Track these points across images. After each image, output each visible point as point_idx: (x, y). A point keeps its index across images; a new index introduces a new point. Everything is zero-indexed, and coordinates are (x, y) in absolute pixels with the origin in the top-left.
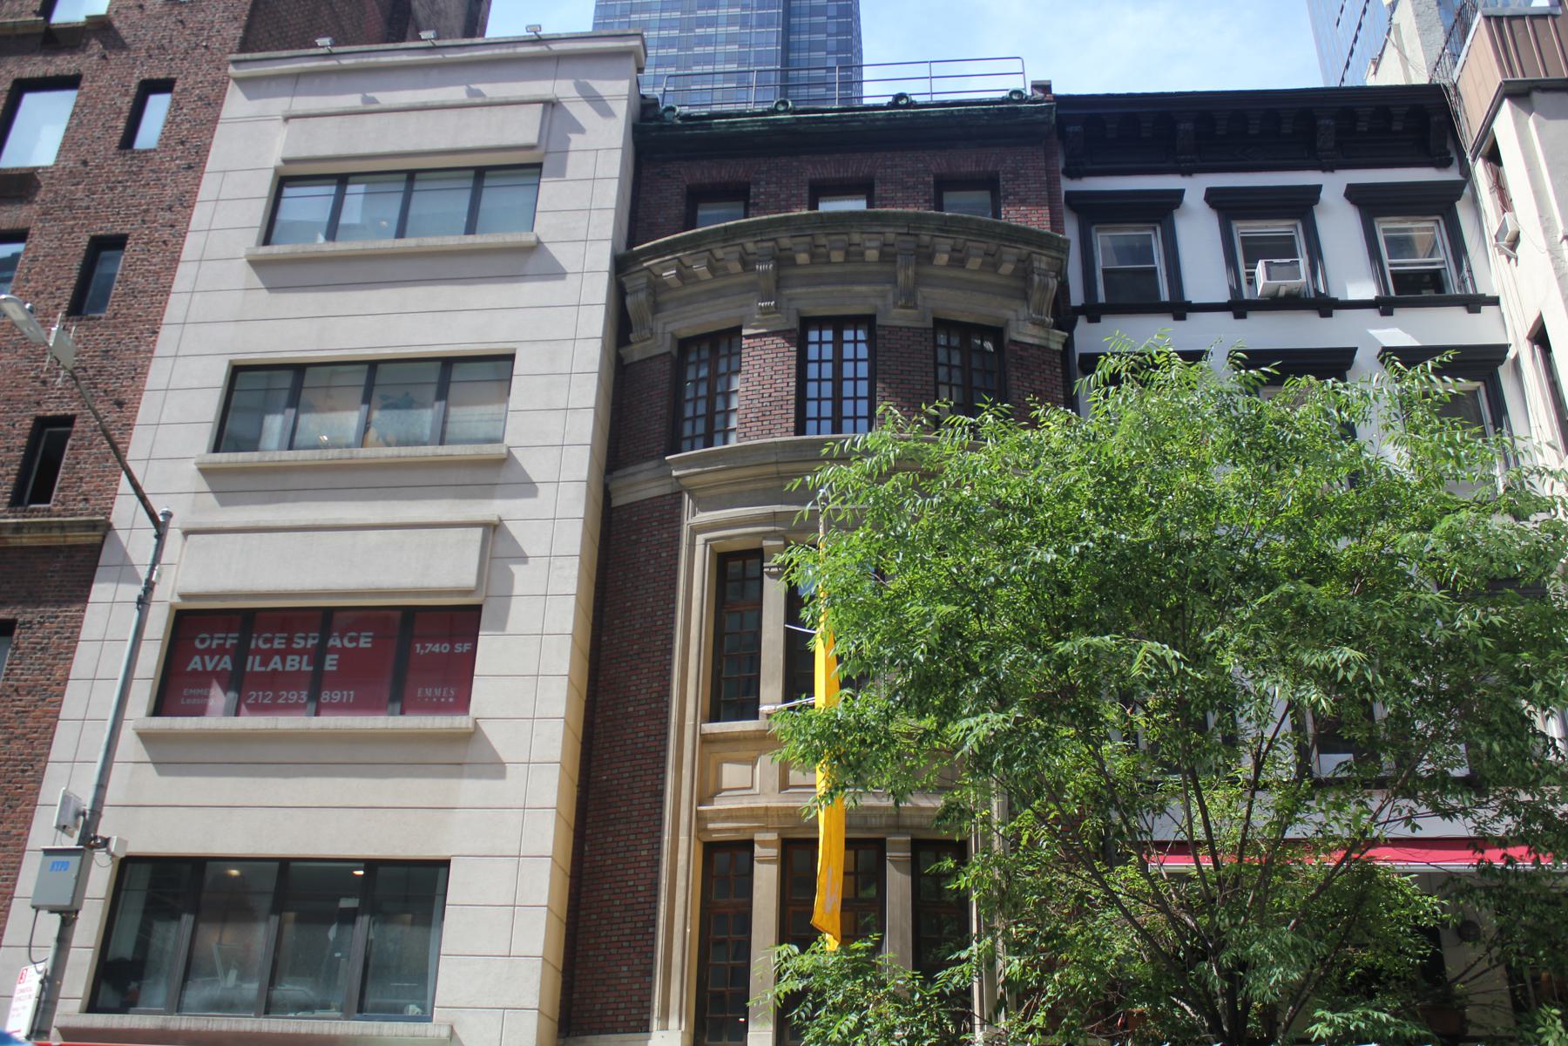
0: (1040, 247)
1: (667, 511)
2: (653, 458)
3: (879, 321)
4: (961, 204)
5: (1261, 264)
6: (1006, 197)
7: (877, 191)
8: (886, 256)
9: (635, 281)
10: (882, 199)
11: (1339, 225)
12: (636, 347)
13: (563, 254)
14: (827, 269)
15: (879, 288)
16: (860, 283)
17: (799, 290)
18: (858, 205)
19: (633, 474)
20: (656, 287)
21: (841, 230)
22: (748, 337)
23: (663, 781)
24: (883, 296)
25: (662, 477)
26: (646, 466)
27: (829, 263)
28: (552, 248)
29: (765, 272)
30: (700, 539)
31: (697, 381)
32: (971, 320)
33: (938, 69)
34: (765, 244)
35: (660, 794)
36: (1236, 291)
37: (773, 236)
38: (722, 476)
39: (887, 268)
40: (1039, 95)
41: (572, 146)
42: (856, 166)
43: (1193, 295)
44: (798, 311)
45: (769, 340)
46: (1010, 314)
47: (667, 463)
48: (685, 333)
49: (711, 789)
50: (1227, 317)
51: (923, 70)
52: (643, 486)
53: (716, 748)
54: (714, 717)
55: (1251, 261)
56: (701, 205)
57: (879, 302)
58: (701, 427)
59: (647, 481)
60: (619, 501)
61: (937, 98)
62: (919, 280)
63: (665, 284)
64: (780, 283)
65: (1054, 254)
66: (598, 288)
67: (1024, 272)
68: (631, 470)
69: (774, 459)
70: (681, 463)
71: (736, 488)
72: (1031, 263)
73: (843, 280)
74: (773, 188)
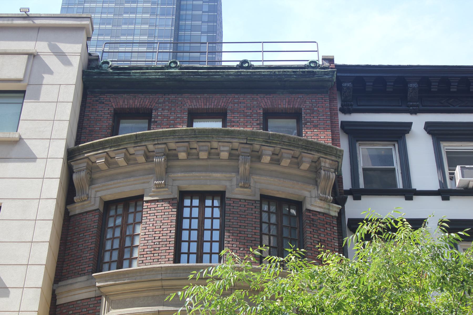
0: (326, 154)
2: (84, 274)
3: (227, 195)
4: (278, 126)
5: (458, 168)
6: (306, 124)
7: (229, 117)
8: (233, 156)
9: (80, 164)
10: (232, 122)
13: (36, 147)
14: (197, 163)
15: (228, 175)
16: (216, 171)
17: (179, 175)
18: (217, 125)
19: (71, 284)
20: (92, 169)
21: (206, 139)
22: (147, 202)
25: (89, 287)
26: (80, 279)
27: (198, 159)
28: (27, 142)
29: (160, 163)
31: (115, 227)
32: (283, 196)
36: (443, 183)
38: (126, 287)
39: (233, 163)
40: (327, 64)
41: (44, 82)
42: (216, 101)
43: (417, 185)
45: (160, 204)
46: (306, 194)
47: (93, 278)
48: (108, 198)
50: (438, 199)
55: (452, 165)
56: (122, 121)
57: (228, 184)
58: (115, 256)
60: (60, 301)
61: (266, 64)
62: (252, 171)
63: (98, 167)
64: (168, 170)
65: (334, 158)
66: (56, 168)
67: (316, 169)
68: (70, 281)
69: (160, 277)
70: (103, 278)
71: (136, 295)
72: (320, 163)
73: (207, 169)
74: (166, 113)
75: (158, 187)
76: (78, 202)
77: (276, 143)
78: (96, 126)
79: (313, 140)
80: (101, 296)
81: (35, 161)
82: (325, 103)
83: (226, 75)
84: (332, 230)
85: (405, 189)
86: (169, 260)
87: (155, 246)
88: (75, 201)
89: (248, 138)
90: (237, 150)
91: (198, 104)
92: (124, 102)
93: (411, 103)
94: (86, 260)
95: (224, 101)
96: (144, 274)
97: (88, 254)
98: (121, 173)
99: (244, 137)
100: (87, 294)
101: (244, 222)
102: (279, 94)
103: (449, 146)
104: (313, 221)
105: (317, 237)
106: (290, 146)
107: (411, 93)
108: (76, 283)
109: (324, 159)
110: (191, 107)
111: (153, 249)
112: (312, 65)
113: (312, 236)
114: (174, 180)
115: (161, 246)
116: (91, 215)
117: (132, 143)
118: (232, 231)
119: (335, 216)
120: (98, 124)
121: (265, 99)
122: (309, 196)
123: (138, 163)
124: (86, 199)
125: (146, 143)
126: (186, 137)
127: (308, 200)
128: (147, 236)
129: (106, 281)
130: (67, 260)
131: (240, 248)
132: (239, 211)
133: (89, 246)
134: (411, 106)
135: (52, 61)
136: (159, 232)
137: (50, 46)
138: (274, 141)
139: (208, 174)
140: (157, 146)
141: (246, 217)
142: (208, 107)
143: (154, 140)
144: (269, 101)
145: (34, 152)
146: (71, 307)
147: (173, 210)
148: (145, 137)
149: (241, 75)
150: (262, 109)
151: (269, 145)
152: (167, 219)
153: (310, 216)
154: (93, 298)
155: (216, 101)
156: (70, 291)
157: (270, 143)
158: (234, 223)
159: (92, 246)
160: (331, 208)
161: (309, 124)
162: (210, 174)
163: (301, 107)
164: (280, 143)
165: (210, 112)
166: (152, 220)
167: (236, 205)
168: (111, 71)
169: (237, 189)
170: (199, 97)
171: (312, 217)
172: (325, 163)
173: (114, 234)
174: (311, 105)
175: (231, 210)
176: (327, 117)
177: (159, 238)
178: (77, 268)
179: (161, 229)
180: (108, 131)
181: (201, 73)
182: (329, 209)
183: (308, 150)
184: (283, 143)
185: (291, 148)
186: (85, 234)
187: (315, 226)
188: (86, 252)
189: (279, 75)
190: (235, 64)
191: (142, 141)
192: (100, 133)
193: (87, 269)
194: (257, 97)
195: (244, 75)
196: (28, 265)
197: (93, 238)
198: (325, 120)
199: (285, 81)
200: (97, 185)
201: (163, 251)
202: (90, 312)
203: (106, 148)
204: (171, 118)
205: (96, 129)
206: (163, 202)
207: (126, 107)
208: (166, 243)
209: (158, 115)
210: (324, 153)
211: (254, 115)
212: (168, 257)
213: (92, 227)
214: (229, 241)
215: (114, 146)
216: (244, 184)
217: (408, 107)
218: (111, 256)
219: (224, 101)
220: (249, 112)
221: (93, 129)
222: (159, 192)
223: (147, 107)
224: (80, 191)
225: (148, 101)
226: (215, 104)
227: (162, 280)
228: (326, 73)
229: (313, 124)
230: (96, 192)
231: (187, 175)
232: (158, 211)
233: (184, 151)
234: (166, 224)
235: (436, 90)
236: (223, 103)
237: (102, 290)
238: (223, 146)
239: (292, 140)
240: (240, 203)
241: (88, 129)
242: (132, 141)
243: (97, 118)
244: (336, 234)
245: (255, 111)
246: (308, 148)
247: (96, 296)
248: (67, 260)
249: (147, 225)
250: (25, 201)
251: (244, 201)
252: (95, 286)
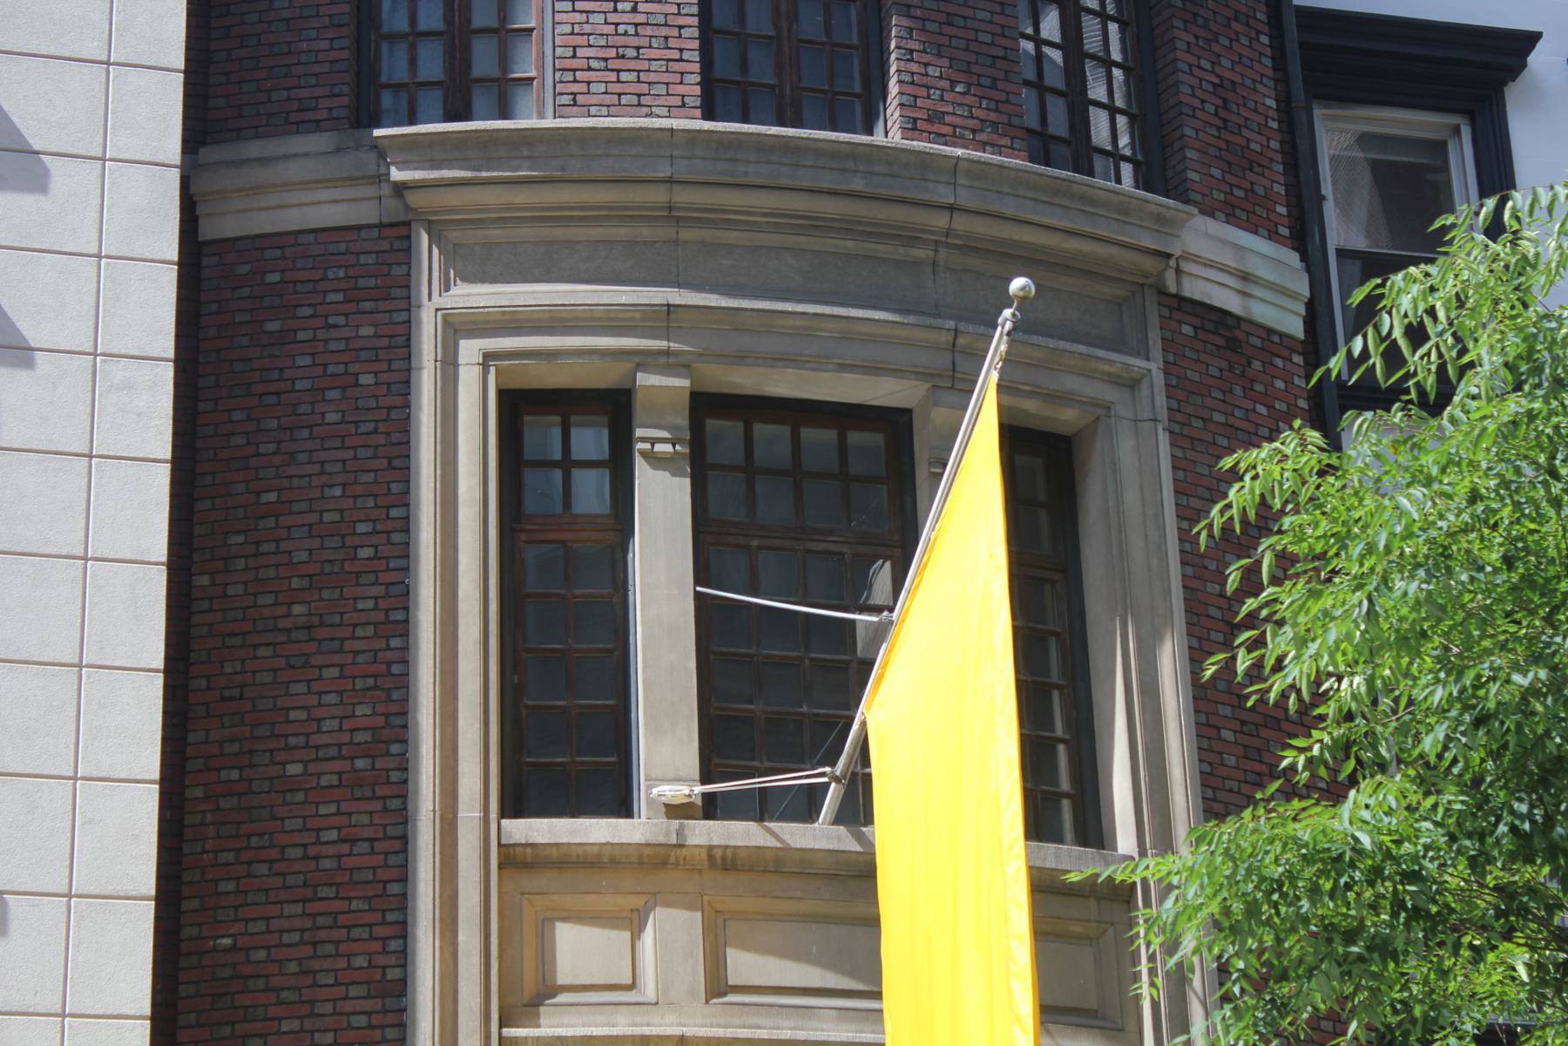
1: (373, 271)
2: (317, 126)
19: (263, 161)
23: (404, 958)
25: (351, 180)
26: (298, 144)
30: (470, 350)
35: (398, 990)
38: (521, 197)
49: (529, 987)
52: (302, 192)
53: (539, 881)
54: (514, 805)
58: (432, 64)
59: (306, 185)
60: (210, 230)
68: (255, 149)
69: (664, 171)
70: (418, 150)
71: (559, 233)
80: (408, 224)
84: (1256, 46)
87: (620, 40)
94: (318, 69)
96: (599, 152)
97: (324, 45)
100: (333, 209)
105: (1207, 66)
108: (286, 157)
111: (612, 53)
113: (1193, 60)
115: (644, 42)
118: (918, 13)
129: (436, 164)
131: (953, 83)
146: (269, 254)
154: (368, 226)
156: (258, 189)
178: (275, 96)
187: (1200, 21)
188: (313, 34)
193: (323, 104)
201: (655, 66)
202: (362, 283)
208: (664, 31)
212: (681, 89)
214: (911, 51)
218: (413, 62)
227: (670, 181)
237: (414, 199)
244: (1268, 62)
247: (385, 220)
252: (382, 178)
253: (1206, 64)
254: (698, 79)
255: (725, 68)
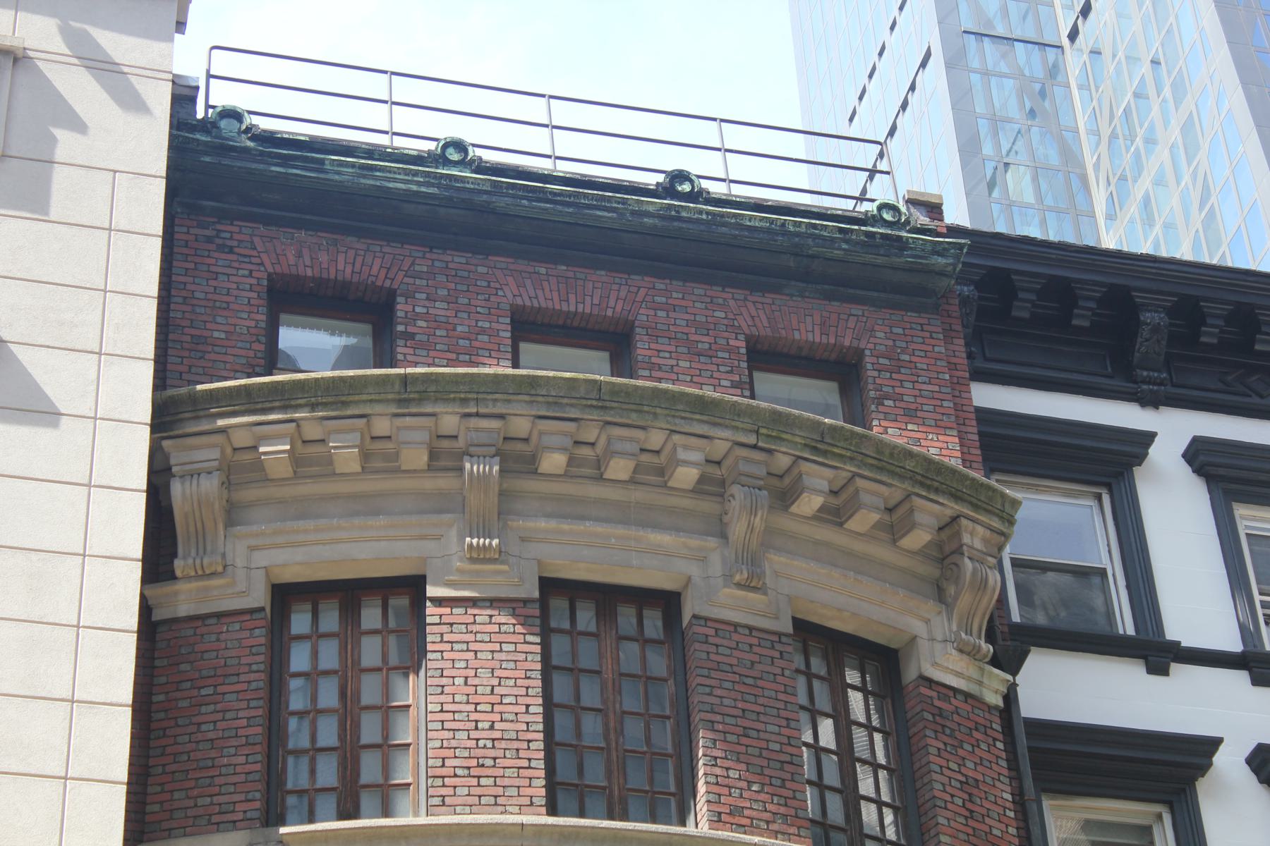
0: (976, 507)
2: (234, 825)
3: (689, 610)
6: (879, 401)
7: (642, 348)
8: (713, 485)
9: (189, 453)
10: (653, 367)
11: (1175, 510)
12: (182, 586)
13: (54, 375)
14: (594, 491)
15: (695, 542)
16: (656, 526)
17: (542, 524)
18: (590, 367)
20: (240, 470)
21: (634, 418)
22: (439, 602)
24: (703, 560)
27: (600, 478)
28: (24, 355)
29: (483, 478)
33: (404, 90)
34: (485, 423)
36: (1248, 633)
37: (500, 409)
39: (707, 506)
40: (922, 219)
41: (60, 154)
42: (597, 294)
44: (539, 562)
45: (483, 615)
46: (918, 628)
50: (1240, 678)
51: (535, 110)
58: (328, 773)
61: (739, 191)
63: (258, 465)
65: (996, 523)
67: (946, 553)
72: (958, 534)
73: (624, 515)
75: (479, 556)
76: (188, 578)
77: (841, 456)
78: (213, 326)
79: (946, 460)
81: (55, 425)
82: (933, 342)
83: (633, 213)
85: (1140, 637)
86: (532, 804)
87: (480, 752)
88: (178, 573)
89: (763, 431)
90: (456, 437)
91: (540, 293)
92: (299, 255)
93: (1145, 373)
94: (235, 779)
95: (623, 294)
97: (242, 759)
98: (335, 497)
99: (749, 426)
101: (752, 699)
102: (792, 295)
103: (1254, 519)
104: (941, 715)
105: (955, 767)
106: (881, 469)
107: (1147, 340)
109: (970, 524)
110: (519, 301)
111: (474, 762)
112: (887, 216)
113: (944, 763)
114: (523, 539)
115: (500, 753)
116: (237, 626)
117: (388, 401)
118: (720, 727)
119: (996, 707)
120: (219, 320)
121: (750, 305)
122: (925, 635)
123: (398, 470)
124: (220, 569)
125: (437, 409)
126: (572, 405)
127: (923, 646)
128: (450, 716)
130: (160, 770)
132: (735, 661)
133: (241, 732)
134: (1144, 382)
135: (77, 87)
136: (489, 708)
137: (68, 35)
138: (836, 450)
139: (633, 532)
140: (474, 422)
141: (759, 683)
142: (572, 309)
143: (464, 401)
144: (761, 312)
145: (48, 391)
147: (530, 638)
148: (433, 388)
149: (680, 219)
150: (742, 337)
151: (820, 460)
152: (512, 665)
153: (931, 698)
155: (598, 293)
157: (825, 453)
158: (726, 702)
159: (251, 731)
160: (985, 681)
161: (890, 403)
162: (641, 533)
163: (862, 346)
164: (851, 459)
165: (575, 324)
166: (463, 664)
167: (725, 642)
168: (250, 144)
169: (727, 590)
170: (543, 271)
171: (937, 703)
172: (971, 534)
173: (314, 699)
174: (890, 343)
175: (712, 657)
176: (943, 390)
177: (492, 728)
178: (200, 802)
179: (496, 699)
180: (256, 346)
181: (554, 193)
182: (980, 683)
183: (929, 488)
184: (860, 457)
185: (884, 479)
186: (220, 689)
187: (948, 731)
188: (232, 751)
189: (798, 234)
190: (652, 180)
191: (422, 398)
192: (230, 351)
193: (239, 807)
194: (724, 295)
195: (689, 220)
196: (66, 778)
197: (253, 703)
198: (936, 395)
199: (813, 257)
200: (255, 528)
201: (508, 772)
203: (297, 408)
204: (459, 328)
205: (216, 334)
206: (491, 607)
207: (309, 273)
208: (516, 745)
209: (418, 316)
210: (971, 504)
211: (720, 354)
212: (529, 791)
213: (246, 669)
214: (716, 758)
215: (325, 405)
216: (751, 576)
217: (1135, 382)
218: (313, 772)
219: (623, 294)
220: (704, 343)
221: (206, 333)
222: (478, 573)
223: (379, 283)
224: (193, 540)
225: (378, 262)
226: (596, 301)
228: (939, 248)
229: (902, 405)
230: (252, 549)
231: (565, 527)
232: (479, 637)
233: (563, 449)
234: (512, 682)
235: (1215, 341)
236: (620, 303)
238: (686, 447)
239: (887, 452)
240: (735, 637)
241: (186, 330)
242: (390, 396)
243: (216, 297)
244: (1004, 764)
245: (723, 342)
246: (929, 482)
248: (160, 770)
249: (444, 681)
250: (33, 555)
251: (747, 632)
253: (954, 766)
254: (544, 783)
255: (562, 692)
